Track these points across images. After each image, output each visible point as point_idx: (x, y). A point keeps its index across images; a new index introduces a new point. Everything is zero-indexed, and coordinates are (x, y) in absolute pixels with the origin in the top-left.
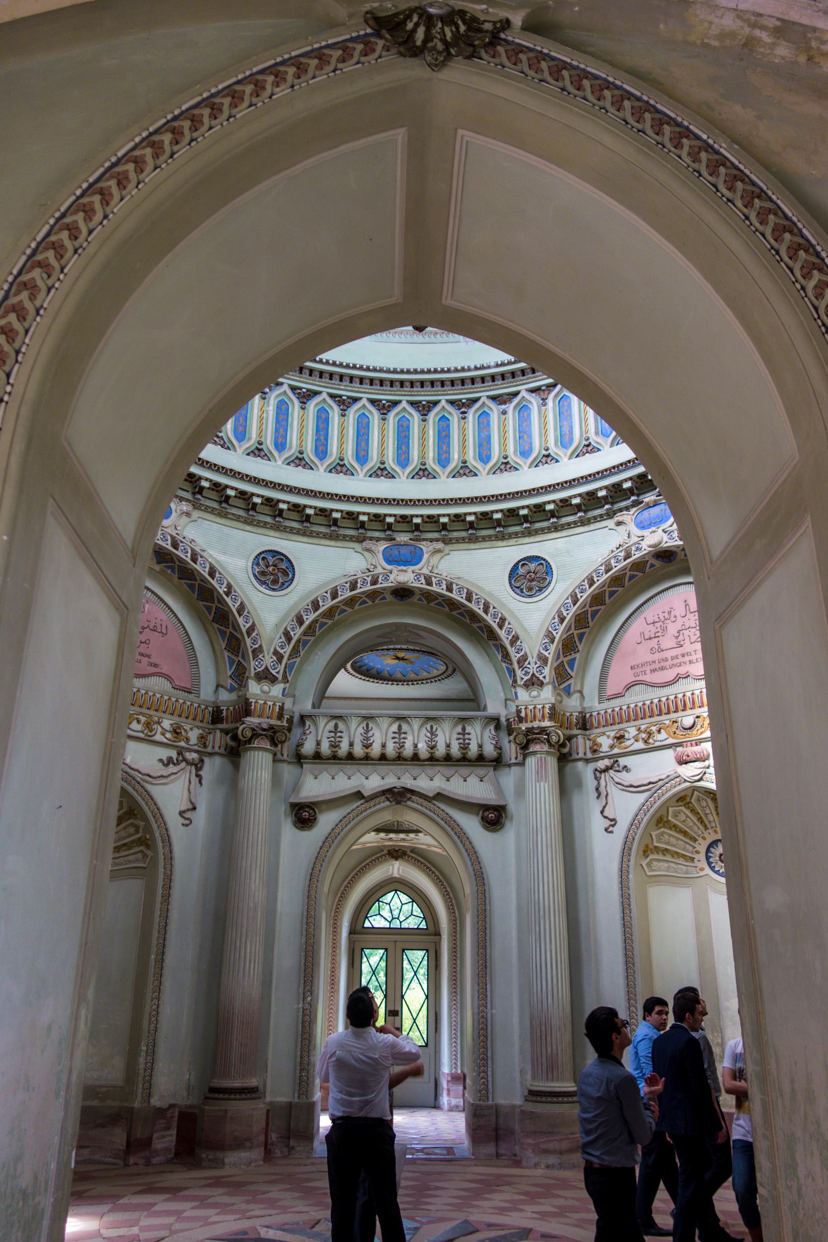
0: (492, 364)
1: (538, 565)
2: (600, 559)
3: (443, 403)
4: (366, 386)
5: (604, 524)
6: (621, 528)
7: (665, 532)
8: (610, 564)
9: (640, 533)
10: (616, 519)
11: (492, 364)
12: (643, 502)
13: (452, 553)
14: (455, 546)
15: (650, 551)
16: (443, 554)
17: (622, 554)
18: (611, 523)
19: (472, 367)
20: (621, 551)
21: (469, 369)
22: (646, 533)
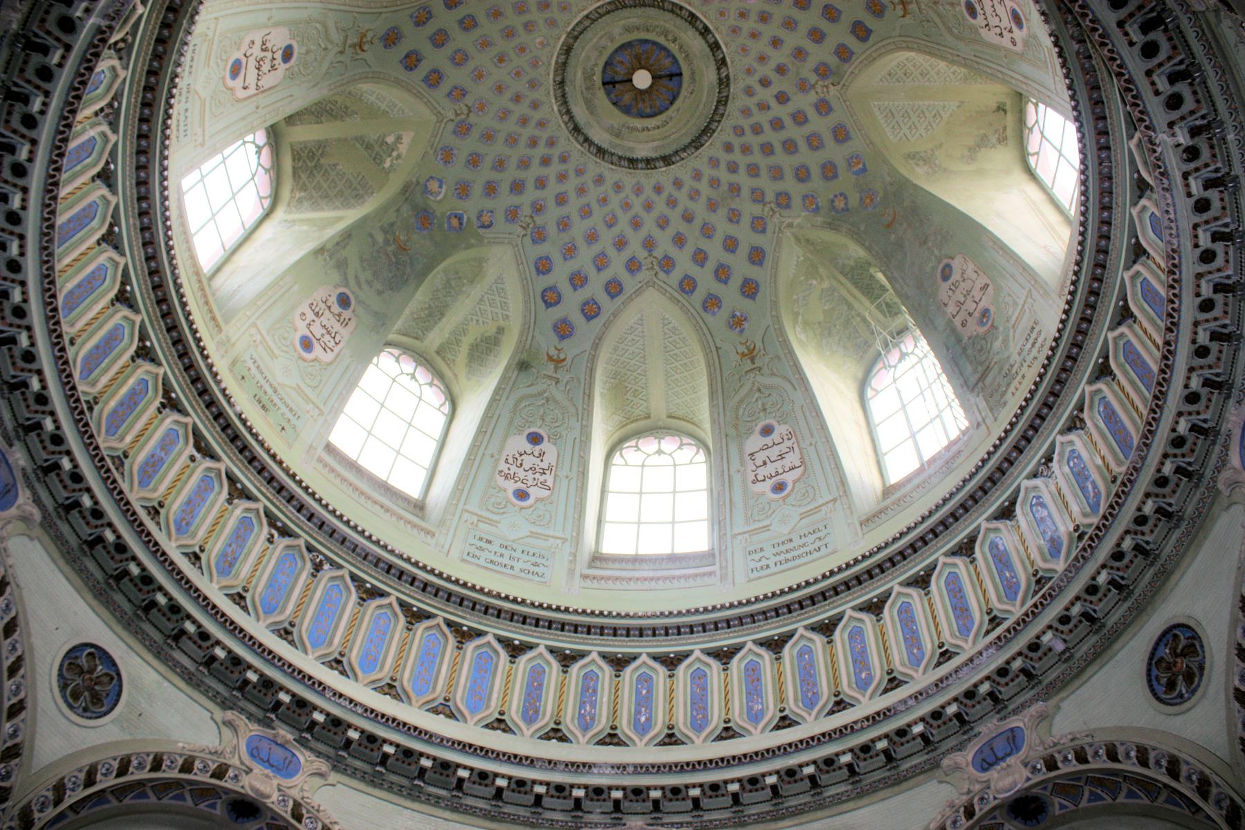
0: (238, 409)
1: (107, 674)
2: (181, 745)
3: (161, 371)
4: (140, 254)
5: (210, 705)
6: (227, 732)
7: (279, 790)
8: (192, 763)
9: (248, 761)
10: (230, 715)
11: (238, 409)
12: (273, 729)
13: (36, 543)
14: (46, 539)
15: (246, 795)
16: (28, 532)
17: (213, 766)
18: (219, 714)
19: (223, 385)
20: (214, 762)
21: (218, 383)
22: (258, 769)
